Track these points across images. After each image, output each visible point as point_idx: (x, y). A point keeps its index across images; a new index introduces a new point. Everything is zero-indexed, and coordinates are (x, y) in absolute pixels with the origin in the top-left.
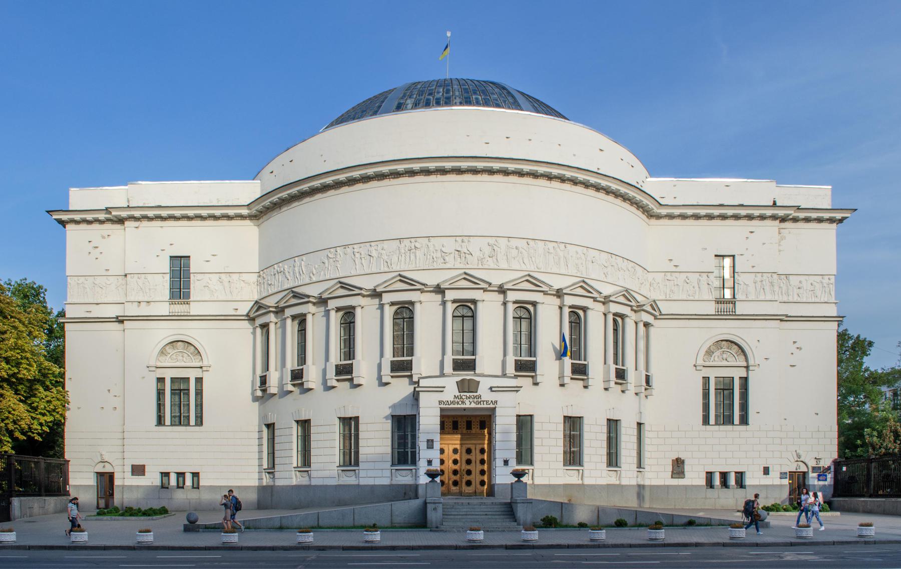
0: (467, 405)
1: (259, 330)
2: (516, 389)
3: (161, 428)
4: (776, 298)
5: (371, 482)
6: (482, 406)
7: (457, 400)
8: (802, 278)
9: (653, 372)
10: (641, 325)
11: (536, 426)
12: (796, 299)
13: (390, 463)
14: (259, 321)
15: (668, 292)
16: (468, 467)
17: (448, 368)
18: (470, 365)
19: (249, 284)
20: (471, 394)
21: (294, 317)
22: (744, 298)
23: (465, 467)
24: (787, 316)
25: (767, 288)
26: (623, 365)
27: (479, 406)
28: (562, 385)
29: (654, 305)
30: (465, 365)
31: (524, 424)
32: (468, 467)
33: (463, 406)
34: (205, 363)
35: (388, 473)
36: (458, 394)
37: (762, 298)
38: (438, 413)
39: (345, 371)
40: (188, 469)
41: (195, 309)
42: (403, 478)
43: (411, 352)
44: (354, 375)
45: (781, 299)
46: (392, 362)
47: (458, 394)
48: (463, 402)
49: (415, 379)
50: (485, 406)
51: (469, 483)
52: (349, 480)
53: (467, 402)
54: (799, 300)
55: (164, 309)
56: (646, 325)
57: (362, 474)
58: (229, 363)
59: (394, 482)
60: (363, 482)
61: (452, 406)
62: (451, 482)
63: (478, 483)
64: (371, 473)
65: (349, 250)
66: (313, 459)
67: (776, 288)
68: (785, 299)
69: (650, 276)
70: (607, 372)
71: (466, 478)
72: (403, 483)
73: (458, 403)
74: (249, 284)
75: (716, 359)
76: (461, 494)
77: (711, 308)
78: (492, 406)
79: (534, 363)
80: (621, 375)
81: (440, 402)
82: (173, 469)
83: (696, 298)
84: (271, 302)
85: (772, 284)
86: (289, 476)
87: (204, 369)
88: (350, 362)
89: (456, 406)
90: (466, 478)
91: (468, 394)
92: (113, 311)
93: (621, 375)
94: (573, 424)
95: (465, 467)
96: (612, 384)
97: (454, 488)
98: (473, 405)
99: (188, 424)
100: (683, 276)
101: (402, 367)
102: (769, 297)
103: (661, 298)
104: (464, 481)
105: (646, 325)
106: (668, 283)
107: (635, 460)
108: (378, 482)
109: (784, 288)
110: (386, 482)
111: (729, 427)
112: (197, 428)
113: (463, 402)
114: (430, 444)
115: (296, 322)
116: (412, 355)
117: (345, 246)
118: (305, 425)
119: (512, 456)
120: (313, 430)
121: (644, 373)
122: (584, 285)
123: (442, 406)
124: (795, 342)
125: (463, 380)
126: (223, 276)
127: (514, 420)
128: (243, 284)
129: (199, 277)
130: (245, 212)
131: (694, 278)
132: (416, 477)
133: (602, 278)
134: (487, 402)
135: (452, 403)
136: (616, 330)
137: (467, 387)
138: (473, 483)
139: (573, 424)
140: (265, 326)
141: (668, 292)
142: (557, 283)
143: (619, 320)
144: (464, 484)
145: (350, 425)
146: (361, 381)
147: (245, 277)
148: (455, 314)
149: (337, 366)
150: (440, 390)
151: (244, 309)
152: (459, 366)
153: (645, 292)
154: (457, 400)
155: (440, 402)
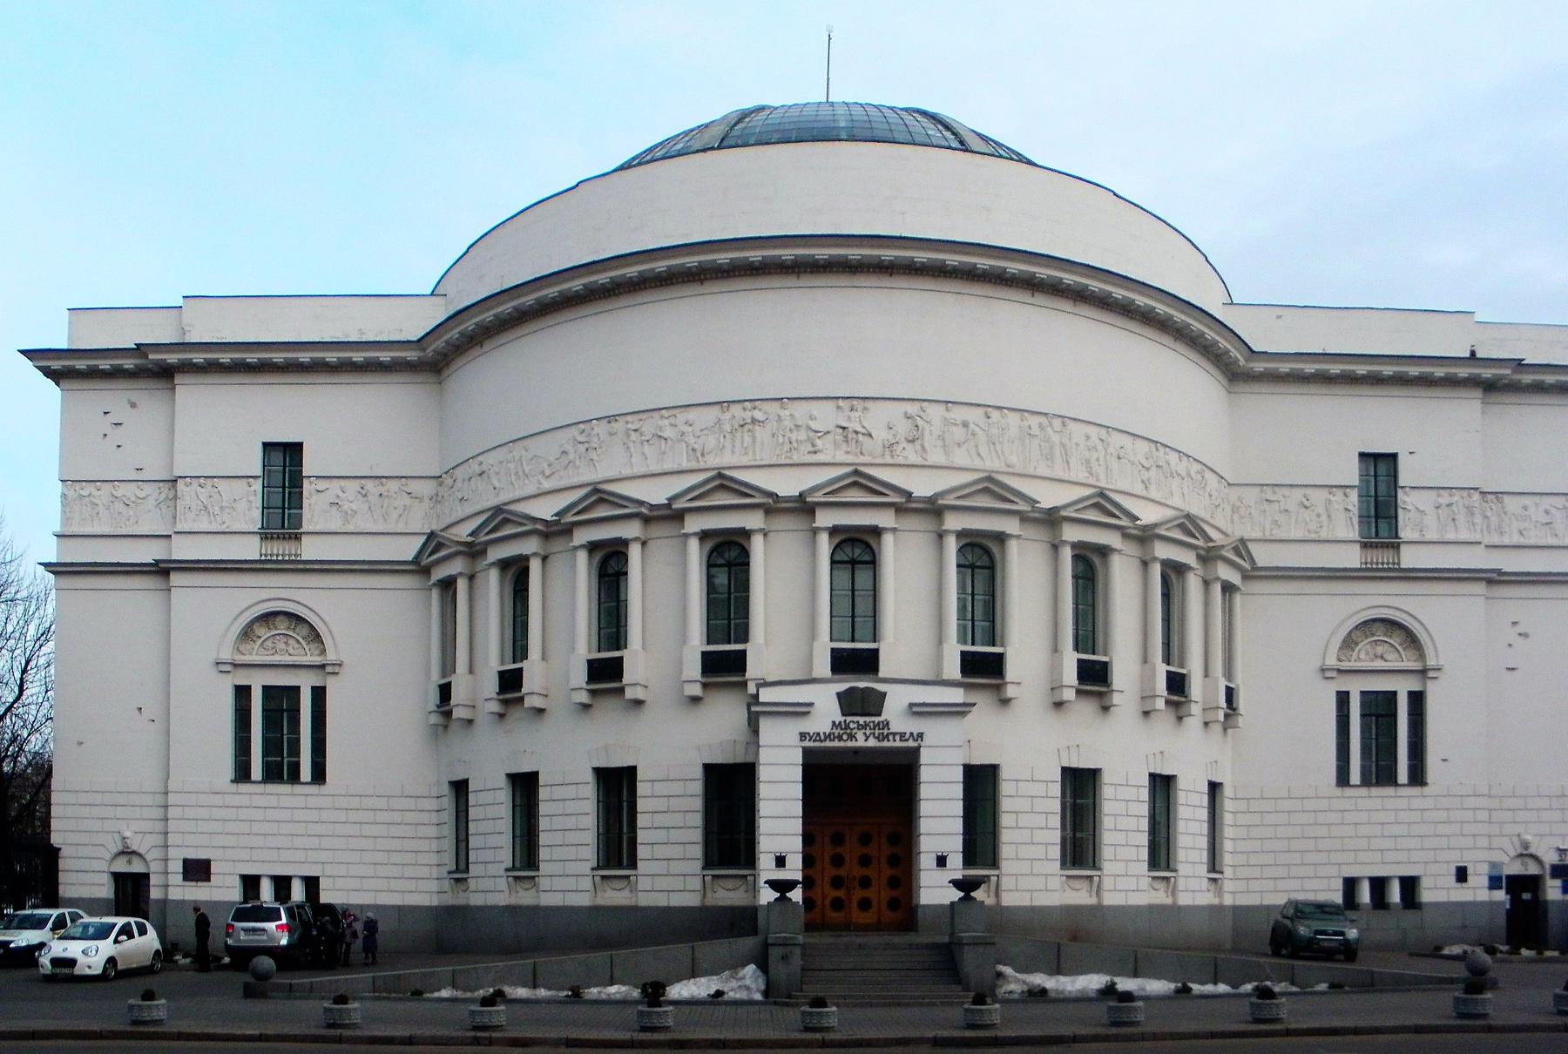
0: (860, 742)
1: (435, 594)
2: (958, 711)
3: (244, 788)
4: (1478, 537)
5: (661, 901)
7: (837, 731)
8: (1527, 501)
9: (1240, 682)
10: (1217, 589)
11: (1006, 788)
12: (1516, 539)
14: (439, 573)
15: (1268, 527)
16: (865, 872)
17: (823, 667)
18: (866, 662)
19: (421, 499)
20: (868, 719)
21: (504, 565)
22: (1415, 536)
23: (858, 872)
24: (1499, 572)
25: (1462, 519)
26: (1182, 666)
27: (885, 744)
28: (1059, 705)
29: (1241, 547)
30: (855, 662)
31: (981, 784)
32: (865, 872)
33: (850, 744)
34: (331, 656)
35: (696, 883)
36: (839, 718)
37: (1451, 536)
38: (798, 758)
39: (605, 673)
40: (295, 869)
41: (311, 549)
42: (728, 895)
43: (744, 636)
44: (625, 680)
45: (1487, 540)
47: (839, 718)
48: (852, 737)
51: (865, 905)
52: (615, 896)
53: (860, 735)
54: (1522, 541)
55: (250, 549)
56: (1228, 588)
57: (644, 883)
58: (373, 656)
59: (710, 902)
60: (645, 900)
61: (828, 744)
62: (827, 902)
63: (884, 904)
64: (661, 883)
65: (619, 426)
66: (544, 854)
67: (1478, 519)
68: (1496, 540)
69: (1234, 493)
70: (1147, 679)
71: (859, 894)
72: (728, 903)
73: (840, 738)
74: (421, 499)
75: (1362, 656)
76: (847, 927)
77: (1352, 557)
80: (1177, 684)
81: (803, 736)
82: (266, 868)
83: (1324, 535)
84: (463, 532)
85: (1470, 511)
86: (492, 885)
87: (329, 669)
88: (616, 654)
89: (836, 744)
90: (859, 894)
91: (862, 720)
92: (147, 553)
93: (1177, 684)
94: (1081, 787)
95: (858, 872)
96: (1160, 704)
97: (834, 915)
98: (872, 743)
99: (294, 777)
100: (1297, 494)
101: (724, 667)
102: (1464, 535)
103: (1257, 534)
104: (855, 899)
105: (1228, 588)
106: (1266, 506)
107: (1205, 856)
108: (677, 901)
109: (1494, 520)
110: (693, 900)
111: (1389, 791)
112: (314, 789)
113: (852, 737)
116: (745, 639)
117: (611, 419)
118: (525, 786)
119: (954, 845)
120: (543, 793)
121: (1223, 684)
122: (1102, 502)
123: (807, 744)
124: (1515, 623)
125: (851, 689)
126: (369, 484)
127: (958, 775)
128: (407, 500)
129: (322, 485)
130: (412, 355)
131: (1318, 497)
132: (755, 890)
133: (1139, 489)
135: (829, 737)
136: (1166, 596)
137: (861, 704)
138: (875, 903)
139: (1081, 787)
140: (448, 585)
141: (1268, 527)
142: (1050, 497)
143: (1173, 577)
144: (855, 905)
145: (617, 787)
146: (639, 693)
147: (414, 486)
148: (837, 558)
149: (590, 663)
150: (801, 711)
151: (407, 550)
152: (845, 662)
153: (1224, 525)
154: (837, 731)
155: (803, 736)
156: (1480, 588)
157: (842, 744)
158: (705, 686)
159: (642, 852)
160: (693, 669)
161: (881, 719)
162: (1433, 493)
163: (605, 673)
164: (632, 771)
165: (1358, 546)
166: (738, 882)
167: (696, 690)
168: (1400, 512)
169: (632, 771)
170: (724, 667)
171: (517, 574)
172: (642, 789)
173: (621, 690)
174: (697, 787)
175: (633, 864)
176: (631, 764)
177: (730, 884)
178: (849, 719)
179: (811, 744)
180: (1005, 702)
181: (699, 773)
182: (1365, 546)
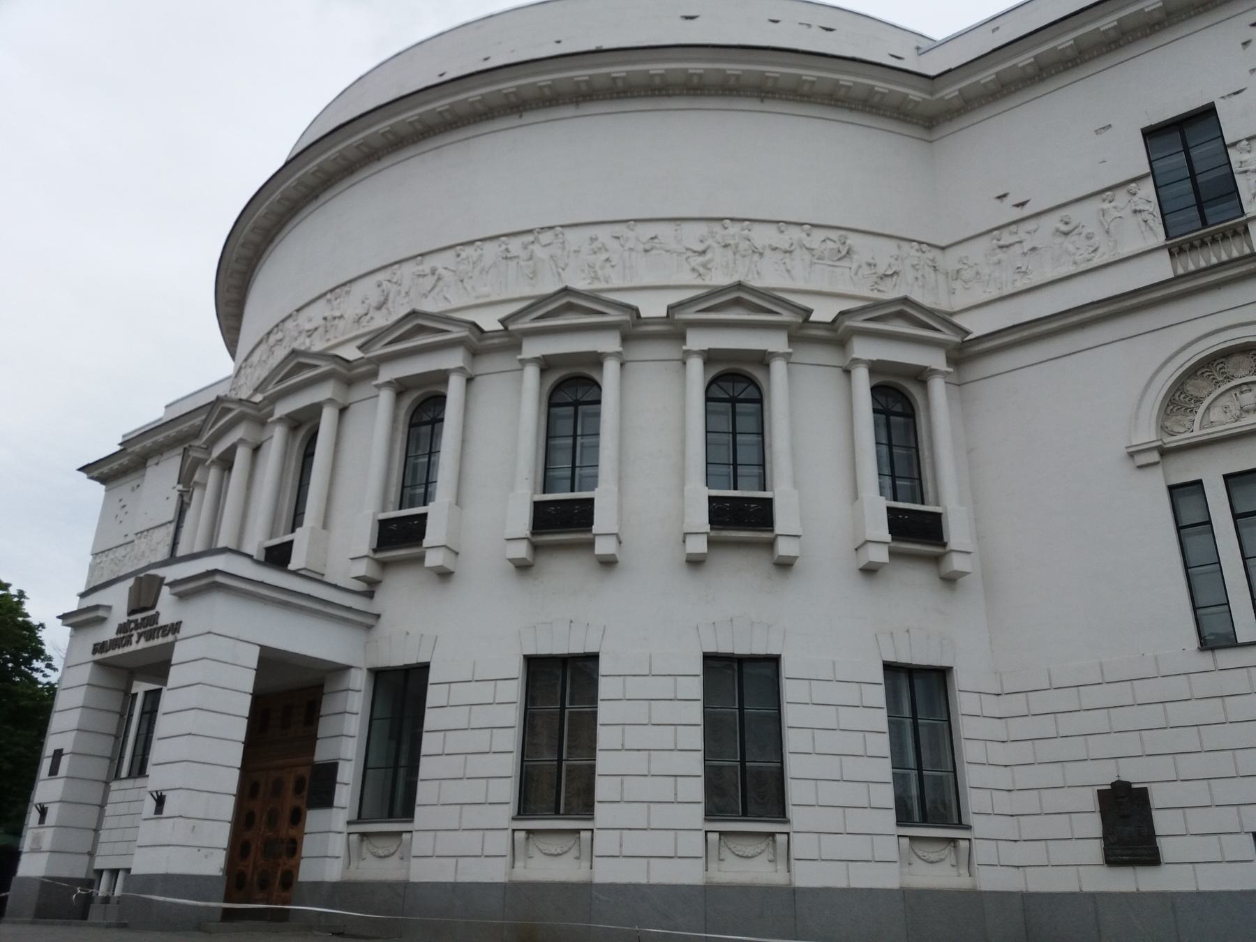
13: (511, 809)
46: (538, 506)
79: (936, 519)
115: (302, 433)
116: (593, 483)
140: (226, 462)
158: (536, 548)
159: (424, 792)
160: (522, 522)
163: (400, 535)
164: (424, 668)
166: (566, 842)
167: (521, 551)
169: (424, 668)
170: (562, 520)
171: (304, 427)
172: (434, 695)
173: (420, 559)
174: (514, 691)
175: (408, 812)
176: (423, 659)
177: (554, 845)
180: (950, 580)
181: (516, 668)
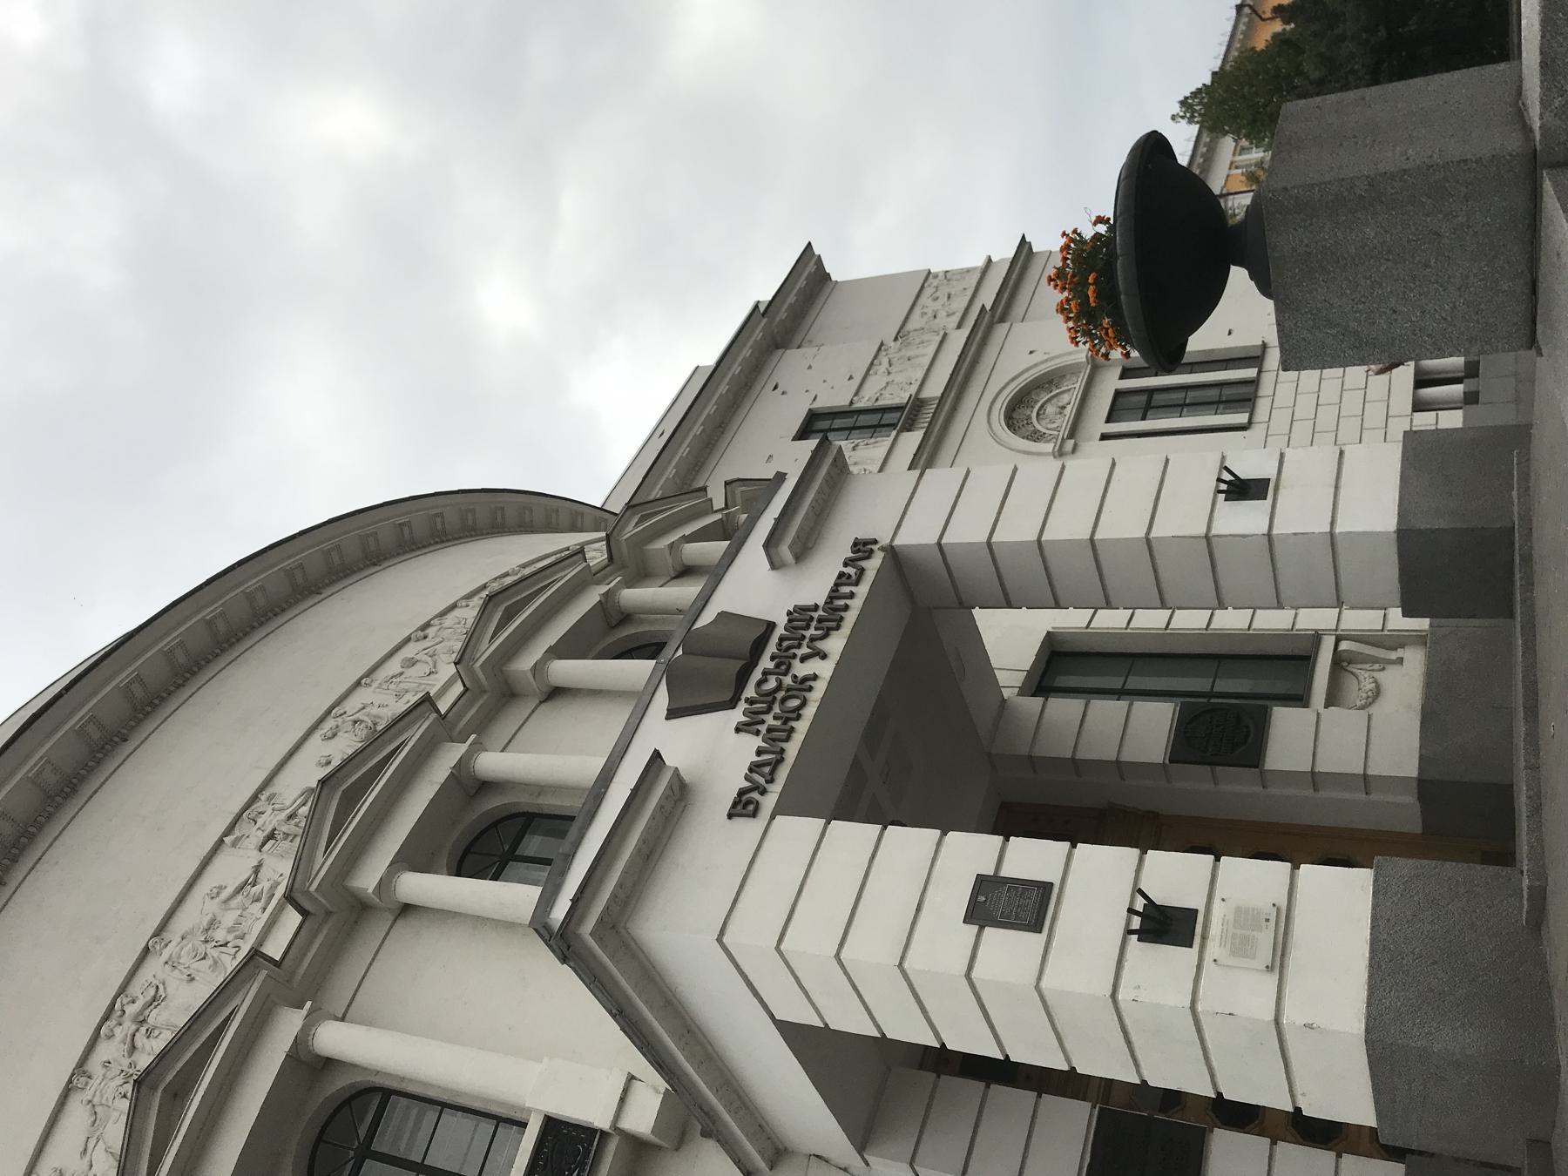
0: (824, 669)
6: (856, 604)
20: (772, 648)
27: (850, 618)
36: (737, 715)
37: (926, 361)
47: (737, 715)
49: (642, 1117)
50: (862, 590)
61: (792, 749)
78: (873, 565)
81: (743, 806)
91: (766, 663)
98: (835, 644)
114: (1008, 905)
123: (769, 802)
134: (842, 579)
135: (777, 739)
156: (1002, 329)
157: (809, 712)
161: (781, 620)
162: (871, 380)
165: (906, 435)
168: (880, 403)
178: (750, 692)
179: (776, 789)
182: (909, 427)
